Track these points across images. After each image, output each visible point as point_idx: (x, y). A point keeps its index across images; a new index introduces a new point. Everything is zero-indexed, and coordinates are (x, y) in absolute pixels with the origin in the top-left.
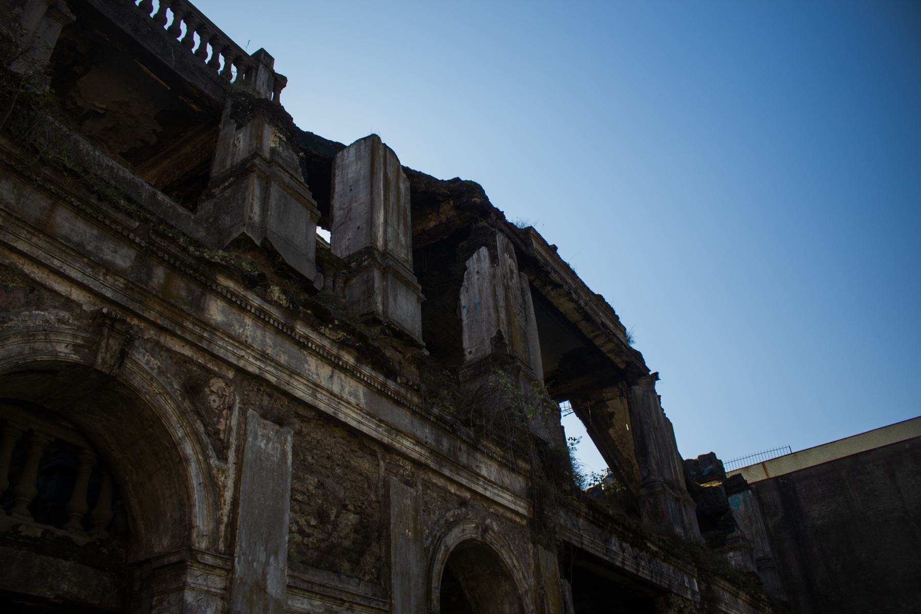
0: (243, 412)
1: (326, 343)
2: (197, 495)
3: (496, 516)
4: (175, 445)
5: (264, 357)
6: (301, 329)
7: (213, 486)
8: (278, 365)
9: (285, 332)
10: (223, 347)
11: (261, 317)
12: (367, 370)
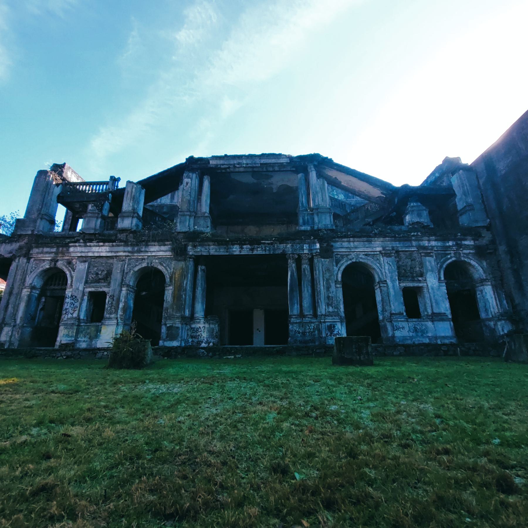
1: (95, 244)
6: (88, 244)
9: (86, 246)
10: (73, 255)
11: (80, 246)
12: (107, 244)
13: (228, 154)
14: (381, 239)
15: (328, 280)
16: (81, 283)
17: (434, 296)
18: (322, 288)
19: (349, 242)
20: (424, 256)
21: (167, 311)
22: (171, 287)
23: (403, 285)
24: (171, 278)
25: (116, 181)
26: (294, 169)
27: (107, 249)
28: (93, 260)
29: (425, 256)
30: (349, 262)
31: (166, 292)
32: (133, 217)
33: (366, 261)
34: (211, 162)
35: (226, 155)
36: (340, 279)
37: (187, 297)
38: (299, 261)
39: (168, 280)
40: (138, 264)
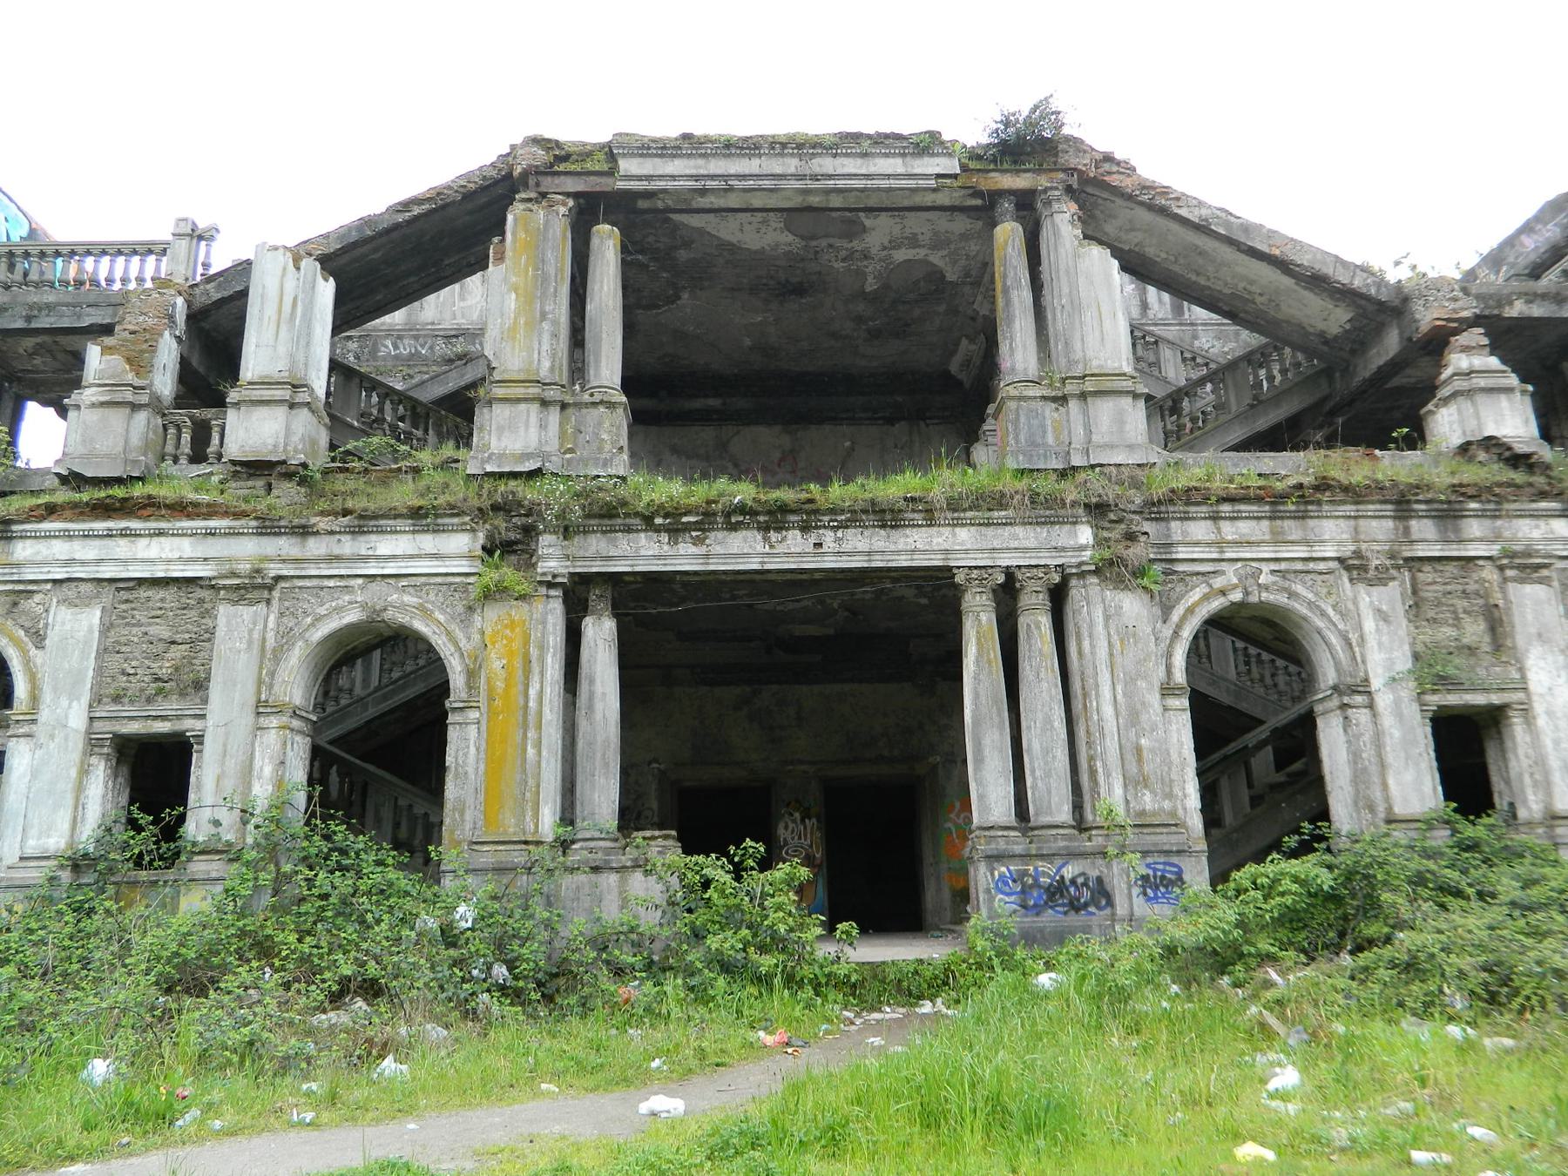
5: (70, 562)
8: (83, 563)
13: (698, 131)
14: (1349, 509)
15: (1130, 681)
16: (73, 697)
17: (1557, 742)
18: (1108, 711)
19: (1215, 518)
20: (1514, 580)
21: (462, 813)
22: (473, 715)
23: (1435, 700)
24: (471, 675)
25: (200, 238)
26: (979, 202)
27: (186, 547)
28: (124, 595)
29: (1522, 581)
30: (1216, 604)
31: (452, 734)
32: (292, 406)
33: (1281, 599)
34: (627, 166)
35: (687, 137)
36: (1180, 677)
37: (544, 753)
38: (1007, 592)
39: (457, 680)
40: (322, 611)
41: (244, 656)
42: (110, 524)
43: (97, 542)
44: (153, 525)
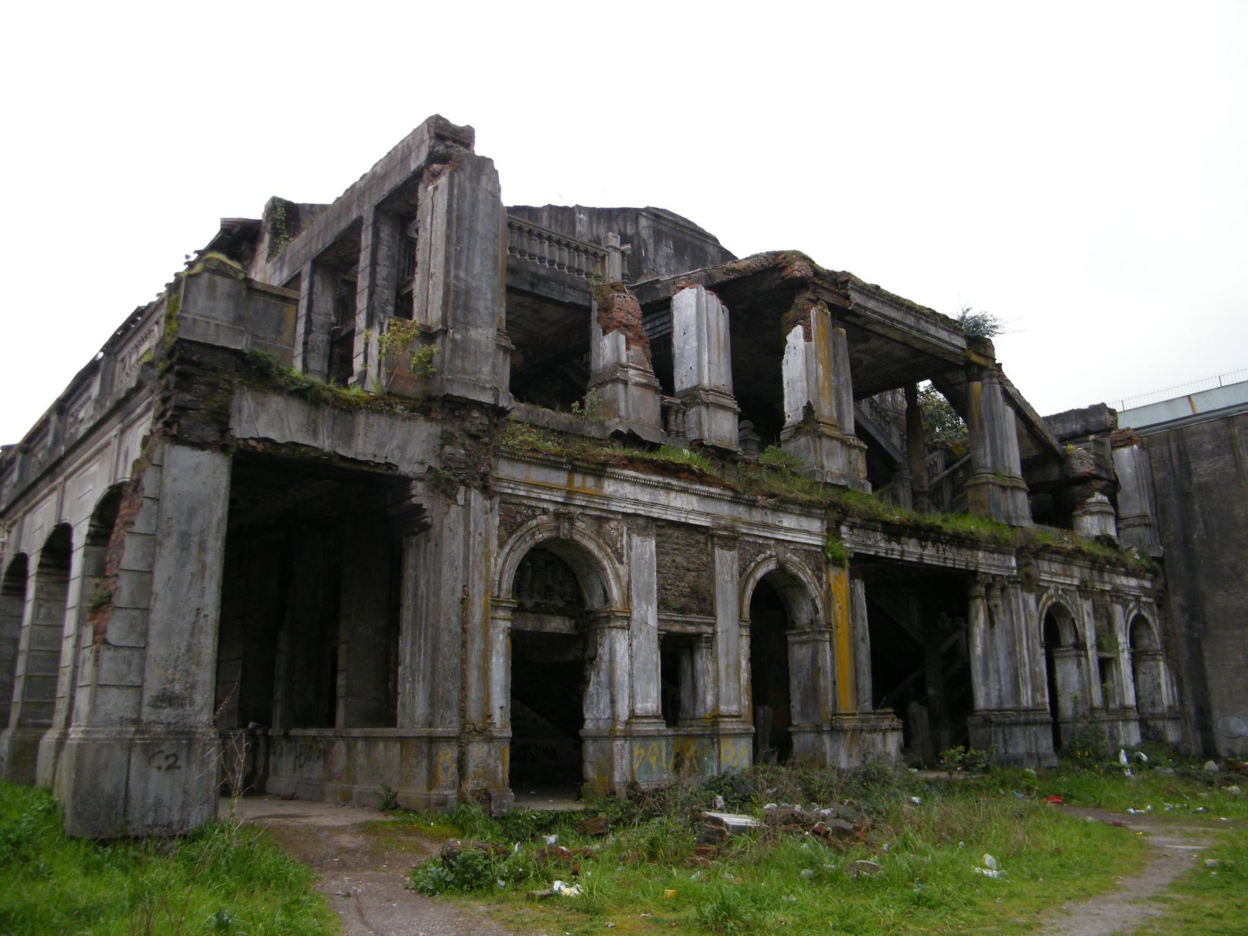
0: (629, 536)
2: (613, 583)
3: (794, 551)
4: (599, 563)
5: (636, 502)
7: (617, 576)
8: (644, 504)
41: (730, 586)
42: (660, 479)
43: (648, 490)
44: (683, 484)
